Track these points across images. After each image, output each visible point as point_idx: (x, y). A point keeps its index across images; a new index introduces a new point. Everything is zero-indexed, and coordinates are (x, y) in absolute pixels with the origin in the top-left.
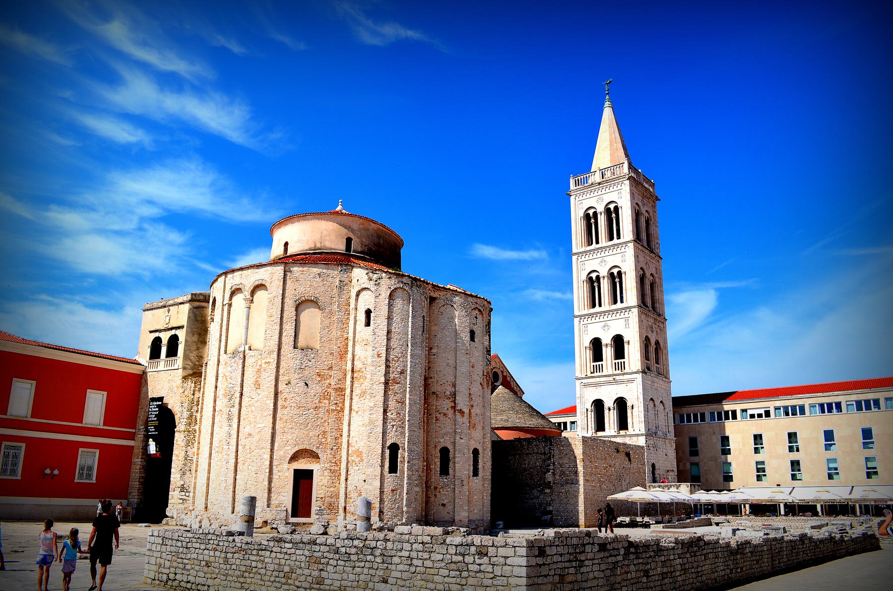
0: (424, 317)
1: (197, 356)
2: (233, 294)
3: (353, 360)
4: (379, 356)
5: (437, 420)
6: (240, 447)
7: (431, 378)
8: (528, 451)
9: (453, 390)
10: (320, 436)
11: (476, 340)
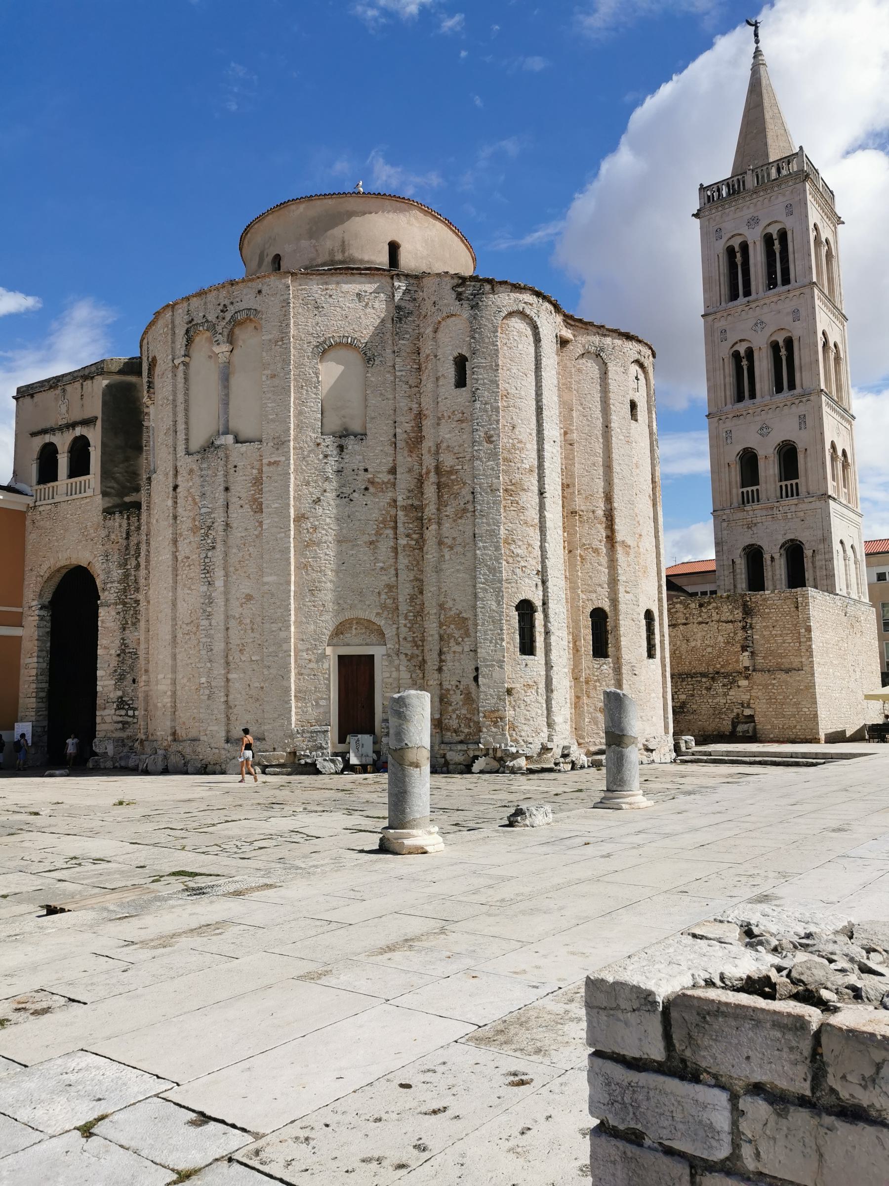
1: (126, 472)
2: (189, 342)
3: (437, 453)
6: (233, 623)
8: (700, 619)
9: (609, 507)
10: (383, 596)
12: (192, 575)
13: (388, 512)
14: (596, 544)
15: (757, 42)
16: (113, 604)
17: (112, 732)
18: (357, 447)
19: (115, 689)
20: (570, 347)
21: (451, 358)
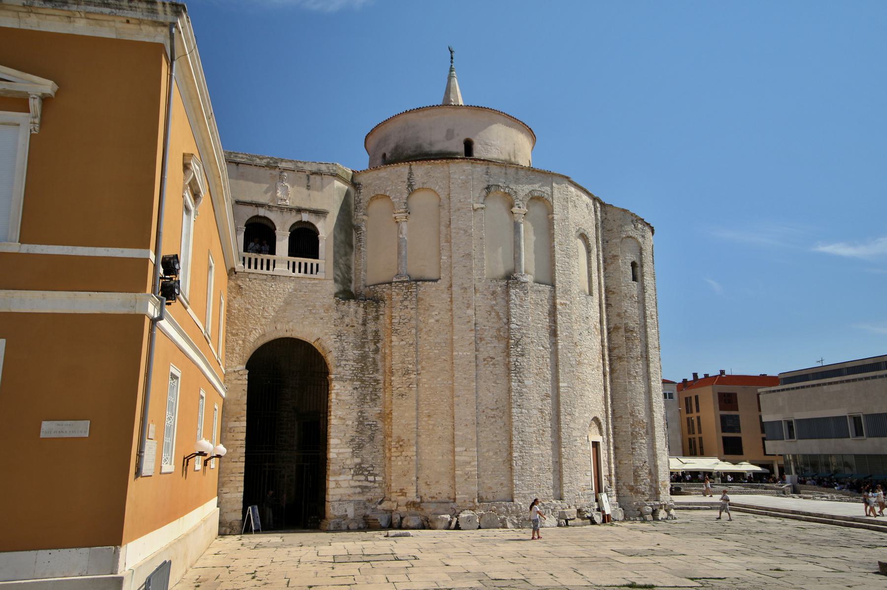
12: (497, 372)
15: (452, 62)
16: (350, 380)
17: (349, 496)
19: (353, 456)
21: (630, 261)
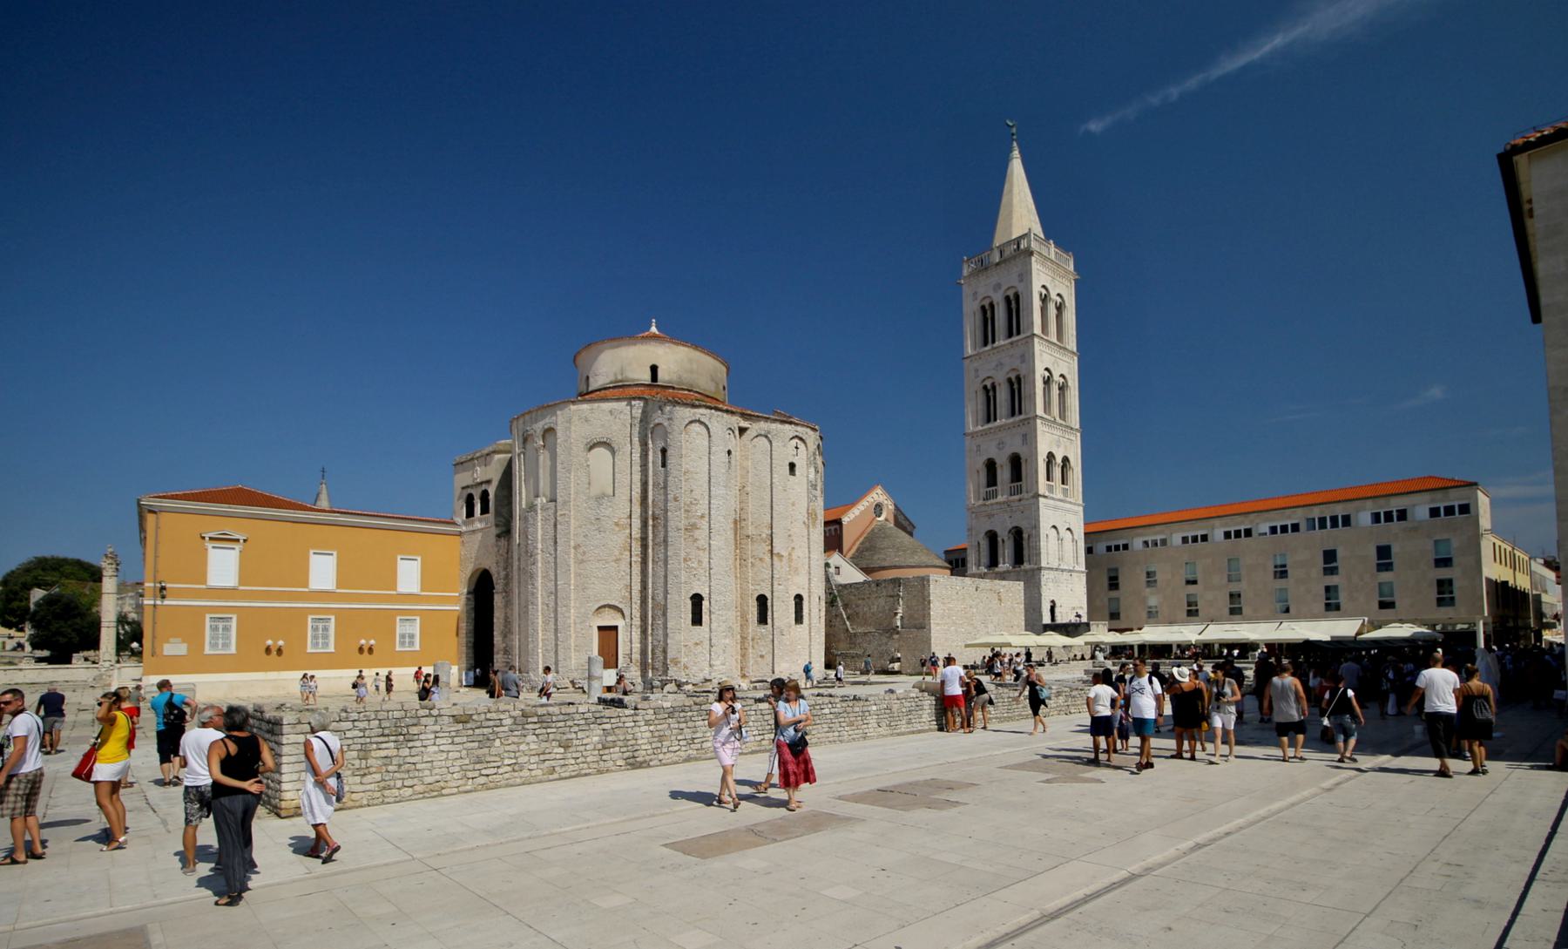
0: (729, 452)
4: (676, 499)
5: (753, 564)
7: (744, 520)
11: (797, 473)
13: (626, 542)
14: (761, 556)
18: (609, 504)
20: (748, 432)
